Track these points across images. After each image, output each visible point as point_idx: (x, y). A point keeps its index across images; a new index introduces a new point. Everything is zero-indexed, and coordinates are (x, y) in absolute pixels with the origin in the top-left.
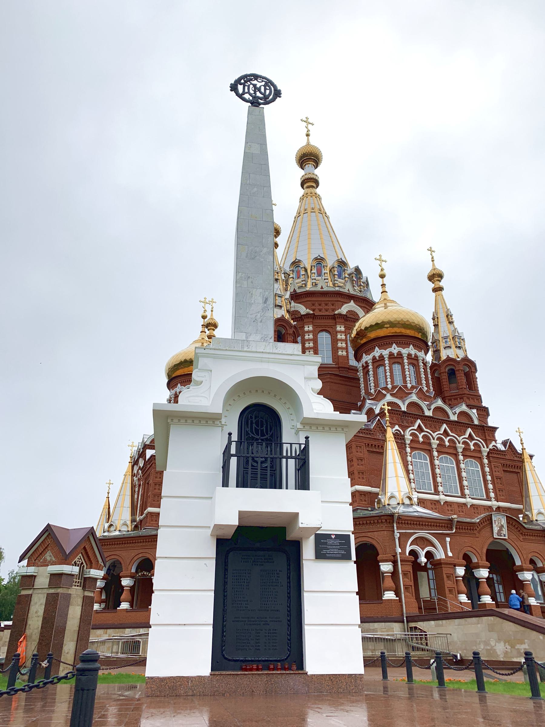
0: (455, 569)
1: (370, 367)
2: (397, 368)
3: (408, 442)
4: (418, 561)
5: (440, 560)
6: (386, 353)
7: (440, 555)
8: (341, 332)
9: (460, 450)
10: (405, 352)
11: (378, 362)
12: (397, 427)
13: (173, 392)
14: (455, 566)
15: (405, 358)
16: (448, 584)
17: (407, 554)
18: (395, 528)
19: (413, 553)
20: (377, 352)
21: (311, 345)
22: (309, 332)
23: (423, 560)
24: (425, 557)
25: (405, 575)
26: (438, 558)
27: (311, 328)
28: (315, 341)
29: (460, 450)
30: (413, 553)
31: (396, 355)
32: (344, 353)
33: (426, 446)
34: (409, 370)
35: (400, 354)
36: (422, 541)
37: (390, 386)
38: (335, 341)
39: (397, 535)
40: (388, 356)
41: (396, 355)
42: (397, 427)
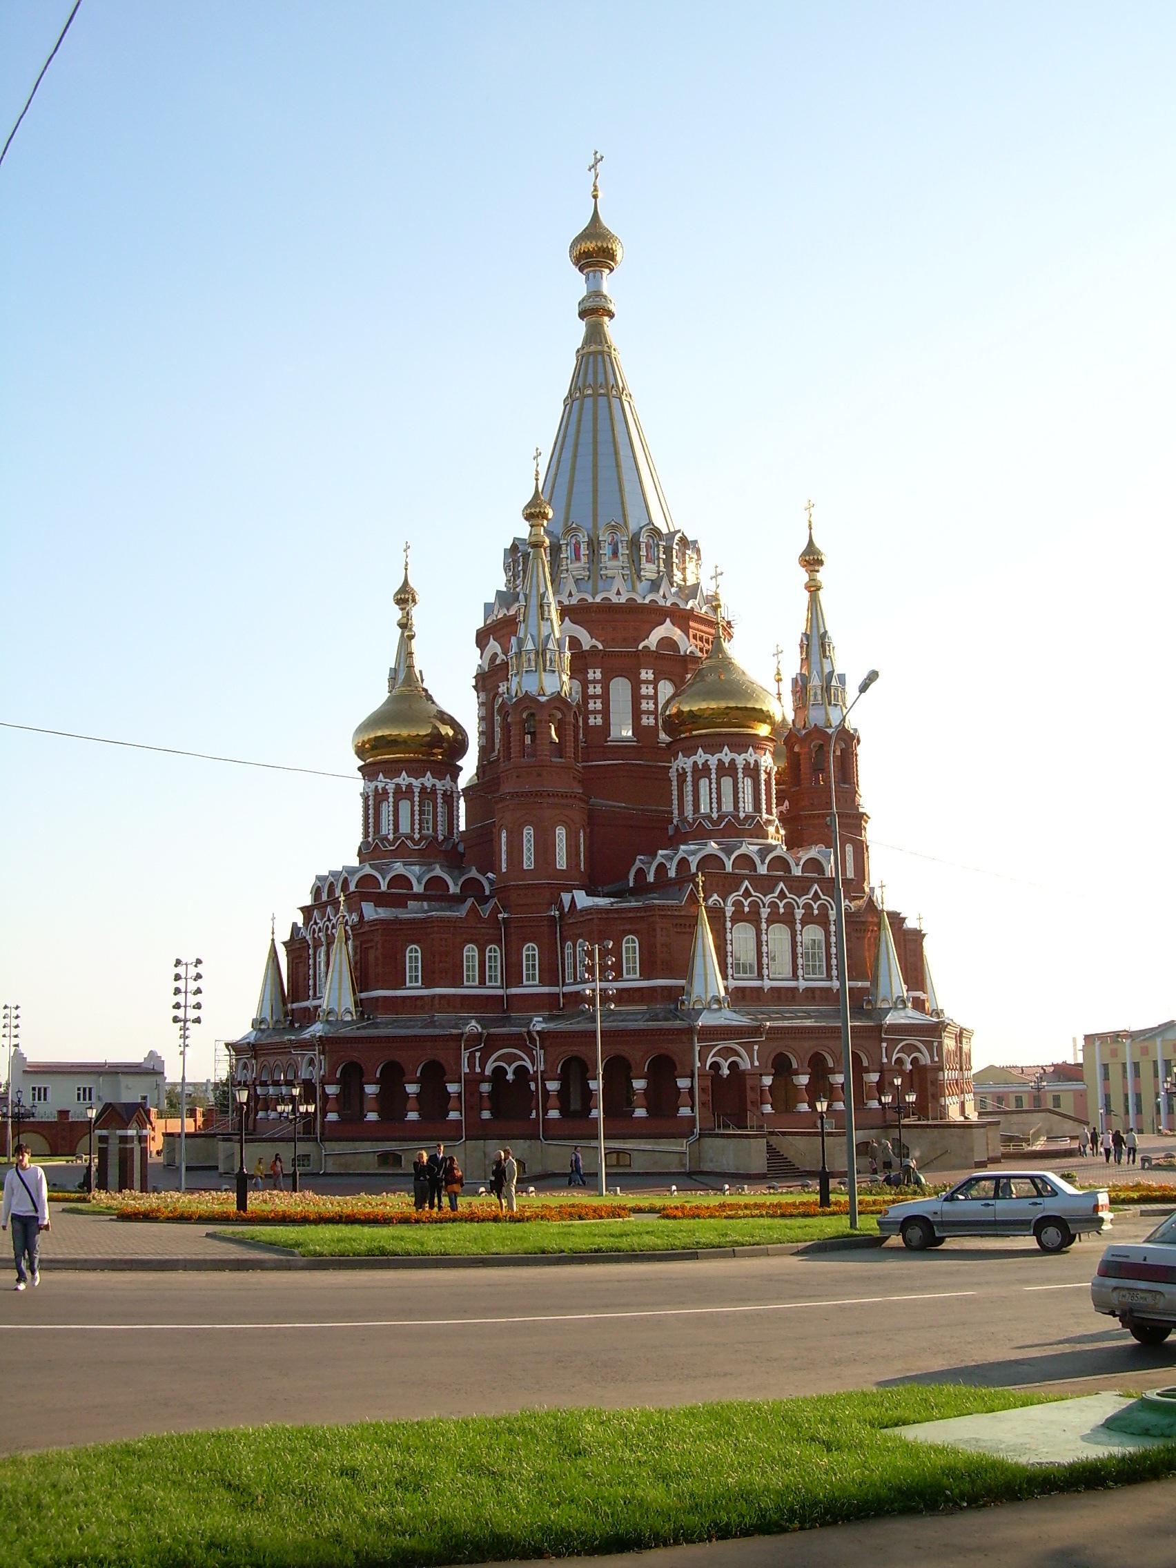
0: (761, 1080)
1: (689, 779)
2: (727, 782)
3: (728, 914)
4: (720, 1072)
5: (744, 1070)
6: (713, 761)
7: (745, 1065)
8: (647, 682)
9: (798, 917)
10: (740, 760)
11: (701, 772)
12: (715, 897)
13: (372, 785)
14: (761, 1075)
15: (740, 770)
16: (750, 1096)
17: (707, 1068)
18: (696, 1041)
19: (716, 1066)
20: (700, 757)
21: (599, 706)
22: (595, 682)
23: (726, 1072)
24: (728, 1069)
25: (703, 1090)
26: (743, 1068)
27: (598, 675)
28: (605, 697)
29: (798, 917)
30: (716, 1066)
31: (727, 765)
32: (652, 721)
33: (753, 918)
34: (747, 785)
35: (733, 761)
36: (727, 1052)
37: (715, 815)
38: (636, 698)
39: (697, 1049)
40: (715, 767)
41: (727, 765)
42: (715, 897)
